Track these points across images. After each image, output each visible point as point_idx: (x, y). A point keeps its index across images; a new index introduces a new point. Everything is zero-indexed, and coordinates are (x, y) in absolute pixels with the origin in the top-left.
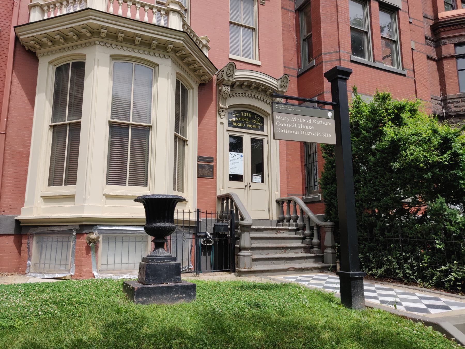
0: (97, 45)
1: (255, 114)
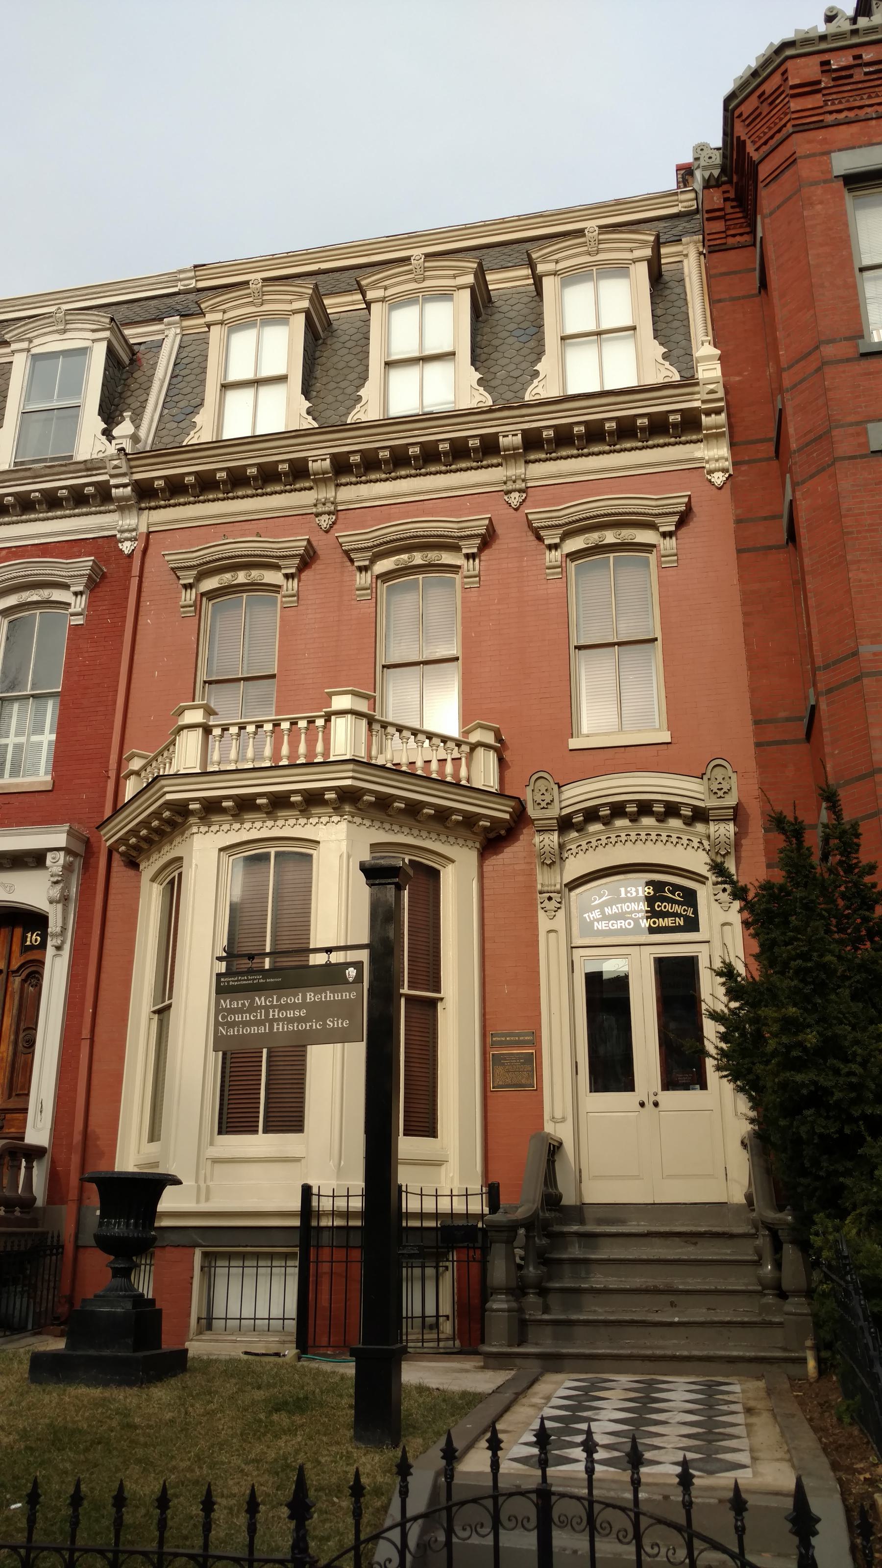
0: (195, 836)
1: (663, 884)
